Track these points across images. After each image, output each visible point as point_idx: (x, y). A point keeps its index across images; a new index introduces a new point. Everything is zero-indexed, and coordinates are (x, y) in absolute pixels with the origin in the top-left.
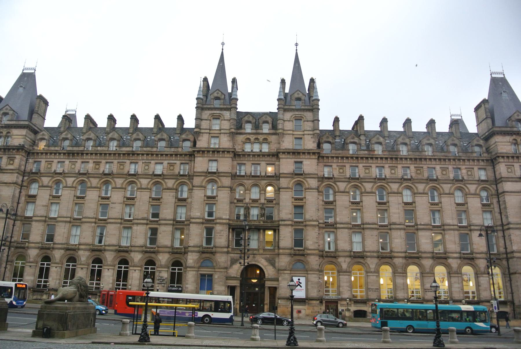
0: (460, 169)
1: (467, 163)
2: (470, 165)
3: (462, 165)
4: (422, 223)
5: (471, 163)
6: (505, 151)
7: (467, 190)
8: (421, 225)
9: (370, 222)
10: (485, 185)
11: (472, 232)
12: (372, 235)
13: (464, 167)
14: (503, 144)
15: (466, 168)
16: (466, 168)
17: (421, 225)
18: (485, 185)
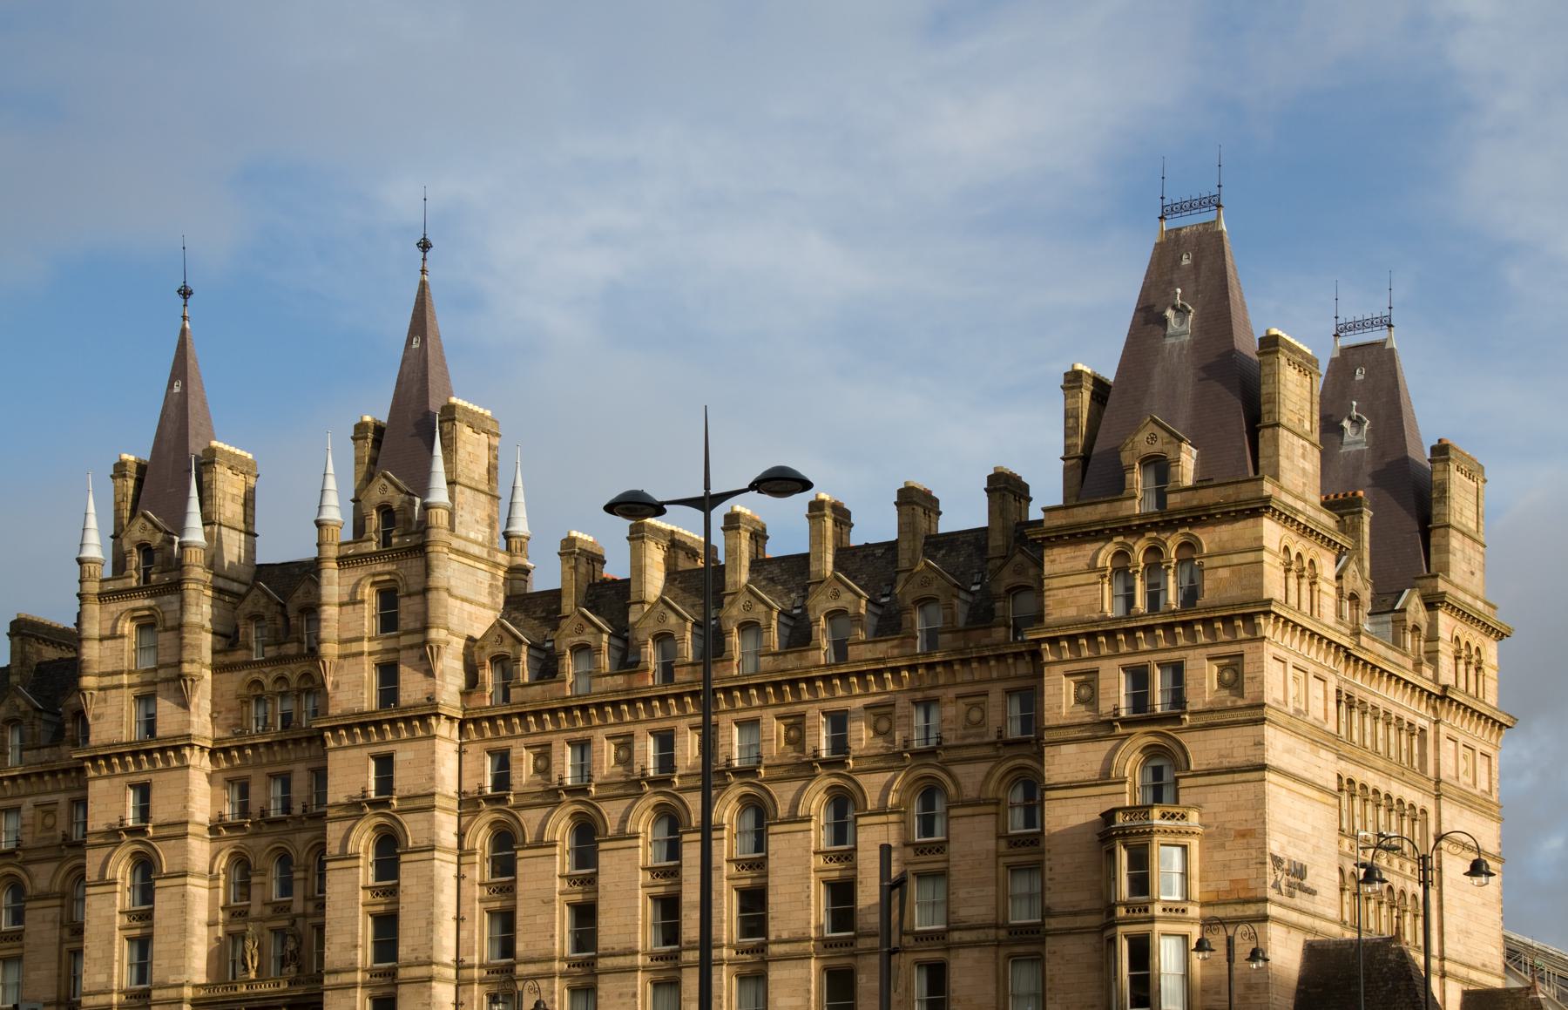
0: (936, 700)
1: (962, 674)
2: (974, 682)
3: (945, 686)
4: (785, 936)
5: (978, 671)
6: (1071, 612)
7: (952, 790)
8: (779, 941)
9: (617, 948)
10: (1019, 761)
11: (953, 953)
12: (620, 995)
13: (951, 693)
14: (1071, 580)
15: (958, 697)
16: (958, 697)
17: (779, 941)
18: (1019, 761)
